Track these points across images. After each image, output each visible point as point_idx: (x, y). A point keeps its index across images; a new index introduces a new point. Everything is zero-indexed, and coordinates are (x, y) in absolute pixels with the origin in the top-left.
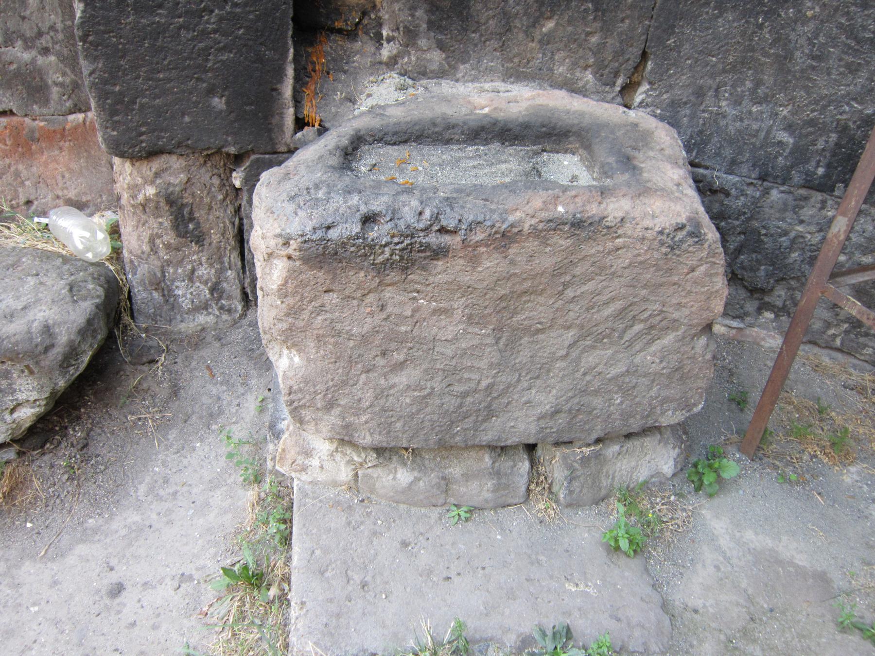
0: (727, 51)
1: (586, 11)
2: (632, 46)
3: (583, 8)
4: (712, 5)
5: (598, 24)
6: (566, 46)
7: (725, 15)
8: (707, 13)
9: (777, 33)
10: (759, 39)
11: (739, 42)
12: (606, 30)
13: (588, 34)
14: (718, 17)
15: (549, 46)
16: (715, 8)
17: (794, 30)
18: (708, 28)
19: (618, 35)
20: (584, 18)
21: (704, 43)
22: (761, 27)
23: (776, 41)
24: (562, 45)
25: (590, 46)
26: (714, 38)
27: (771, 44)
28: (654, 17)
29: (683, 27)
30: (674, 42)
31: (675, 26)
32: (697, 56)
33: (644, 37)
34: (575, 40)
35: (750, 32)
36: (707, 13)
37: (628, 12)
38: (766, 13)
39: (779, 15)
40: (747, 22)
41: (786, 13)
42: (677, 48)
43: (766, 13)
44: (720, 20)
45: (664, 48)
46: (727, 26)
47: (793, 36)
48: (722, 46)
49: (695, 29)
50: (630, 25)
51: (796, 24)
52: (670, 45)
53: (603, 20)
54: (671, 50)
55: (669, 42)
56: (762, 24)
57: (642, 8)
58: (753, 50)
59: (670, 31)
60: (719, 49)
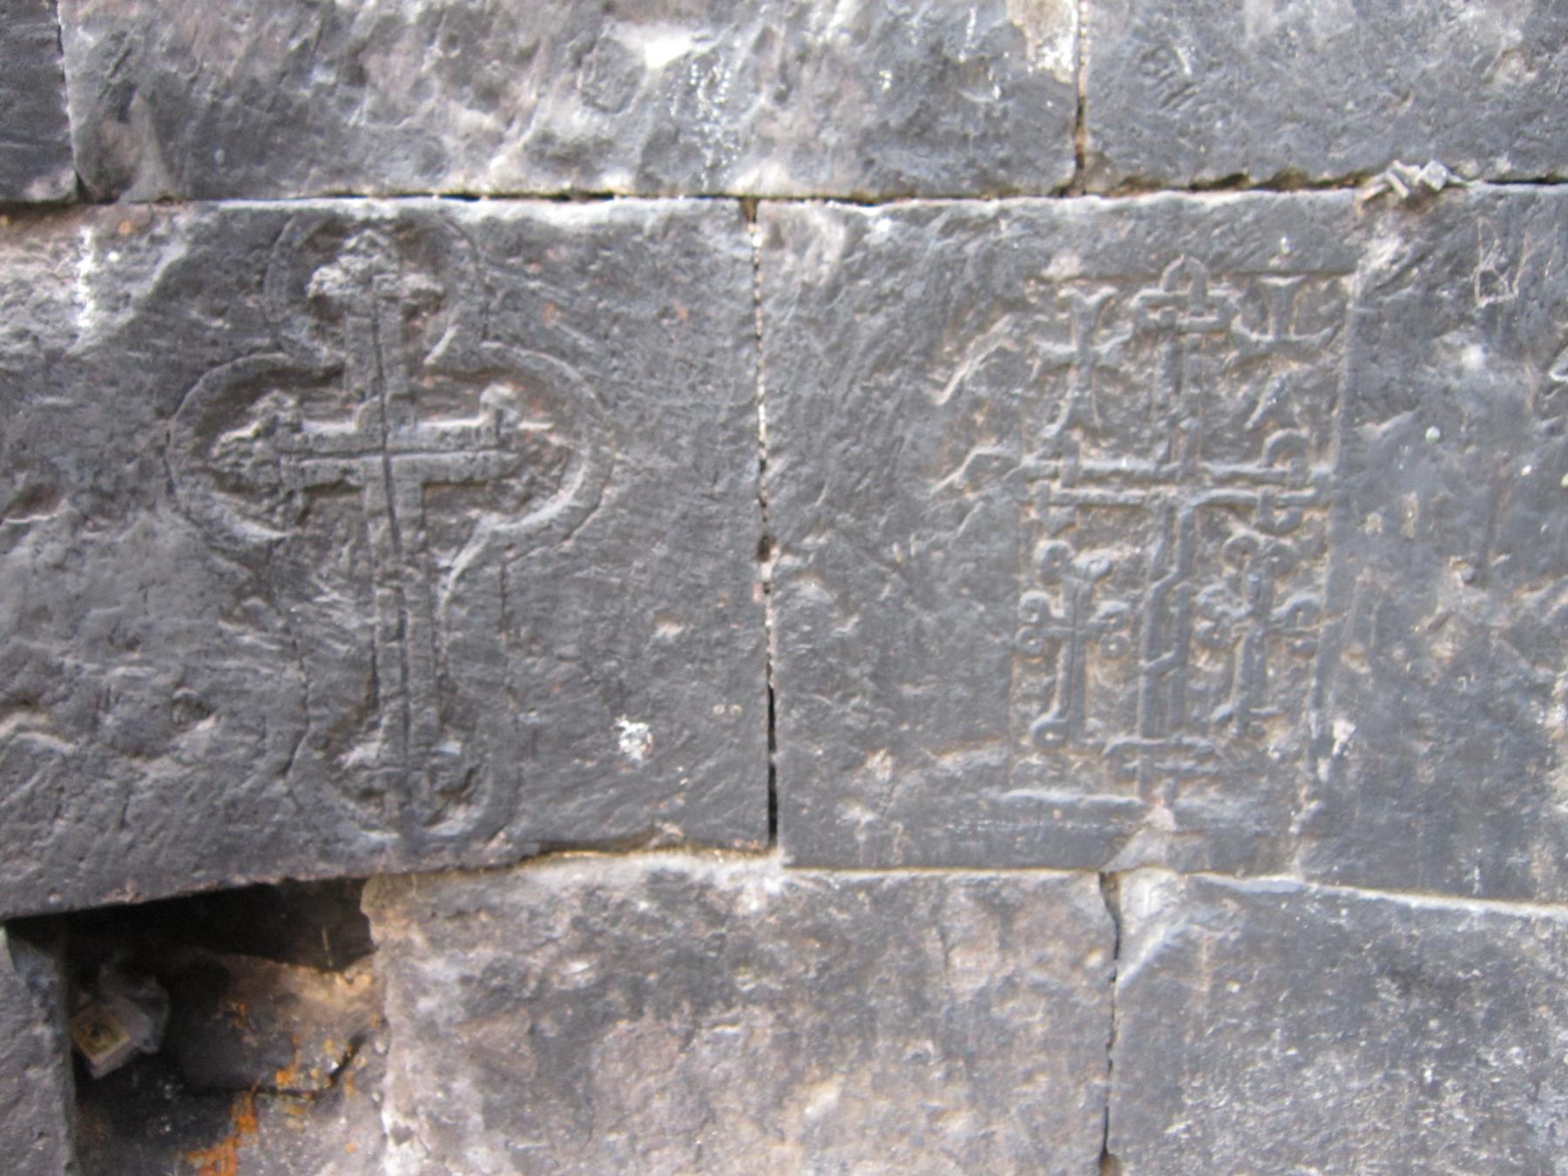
0: (1346, 1152)
1: (920, 1058)
2: (1066, 1139)
3: (910, 1052)
4: (1277, 1035)
5: (960, 1090)
6: (877, 1148)
7: (1320, 1059)
8: (1267, 1056)
9: (1485, 1108)
10: (1437, 1122)
11: (1377, 1130)
12: (986, 1099)
13: (936, 1115)
14: (1298, 1067)
15: (831, 1152)
16: (1289, 1042)
17: (1533, 1099)
18: (1276, 1094)
19: (1021, 1113)
20: (918, 1079)
21: (1273, 1131)
22: (1434, 1090)
23: (1486, 1131)
24: (866, 1147)
25: (948, 1145)
26: (1300, 1120)
27: (1475, 1135)
28: (1117, 1067)
29: (1202, 1090)
30: (1188, 1129)
31: (1180, 1090)
32: (1260, 1164)
33: (1096, 1120)
34: (903, 1133)
35: (1403, 1104)
36: (1267, 1056)
37: (1042, 1058)
38: (1440, 1055)
39: (1486, 1063)
40: (1387, 1078)
41: (1500, 1056)
42: (1200, 1143)
43: (1440, 1055)
44: (1308, 1072)
45: (1159, 1145)
46: (1333, 1089)
47: (1535, 1117)
48: (1329, 1140)
49: (1238, 1095)
50: (1051, 1091)
51: (1537, 1085)
52: (1176, 1137)
53: (970, 1078)
54: (1181, 1150)
55: (1171, 1130)
56: (1435, 1085)
57: (1075, 1048)
58: (1423, 1150)
59: (1168, 1103)
60: (1322, 1145)
